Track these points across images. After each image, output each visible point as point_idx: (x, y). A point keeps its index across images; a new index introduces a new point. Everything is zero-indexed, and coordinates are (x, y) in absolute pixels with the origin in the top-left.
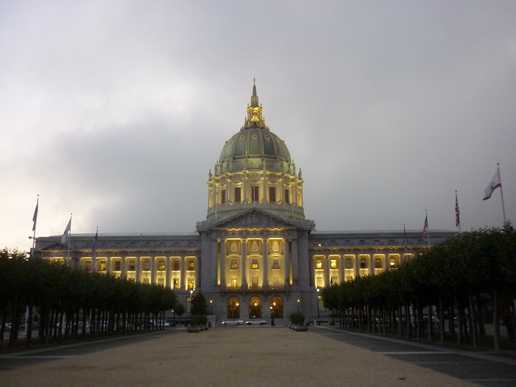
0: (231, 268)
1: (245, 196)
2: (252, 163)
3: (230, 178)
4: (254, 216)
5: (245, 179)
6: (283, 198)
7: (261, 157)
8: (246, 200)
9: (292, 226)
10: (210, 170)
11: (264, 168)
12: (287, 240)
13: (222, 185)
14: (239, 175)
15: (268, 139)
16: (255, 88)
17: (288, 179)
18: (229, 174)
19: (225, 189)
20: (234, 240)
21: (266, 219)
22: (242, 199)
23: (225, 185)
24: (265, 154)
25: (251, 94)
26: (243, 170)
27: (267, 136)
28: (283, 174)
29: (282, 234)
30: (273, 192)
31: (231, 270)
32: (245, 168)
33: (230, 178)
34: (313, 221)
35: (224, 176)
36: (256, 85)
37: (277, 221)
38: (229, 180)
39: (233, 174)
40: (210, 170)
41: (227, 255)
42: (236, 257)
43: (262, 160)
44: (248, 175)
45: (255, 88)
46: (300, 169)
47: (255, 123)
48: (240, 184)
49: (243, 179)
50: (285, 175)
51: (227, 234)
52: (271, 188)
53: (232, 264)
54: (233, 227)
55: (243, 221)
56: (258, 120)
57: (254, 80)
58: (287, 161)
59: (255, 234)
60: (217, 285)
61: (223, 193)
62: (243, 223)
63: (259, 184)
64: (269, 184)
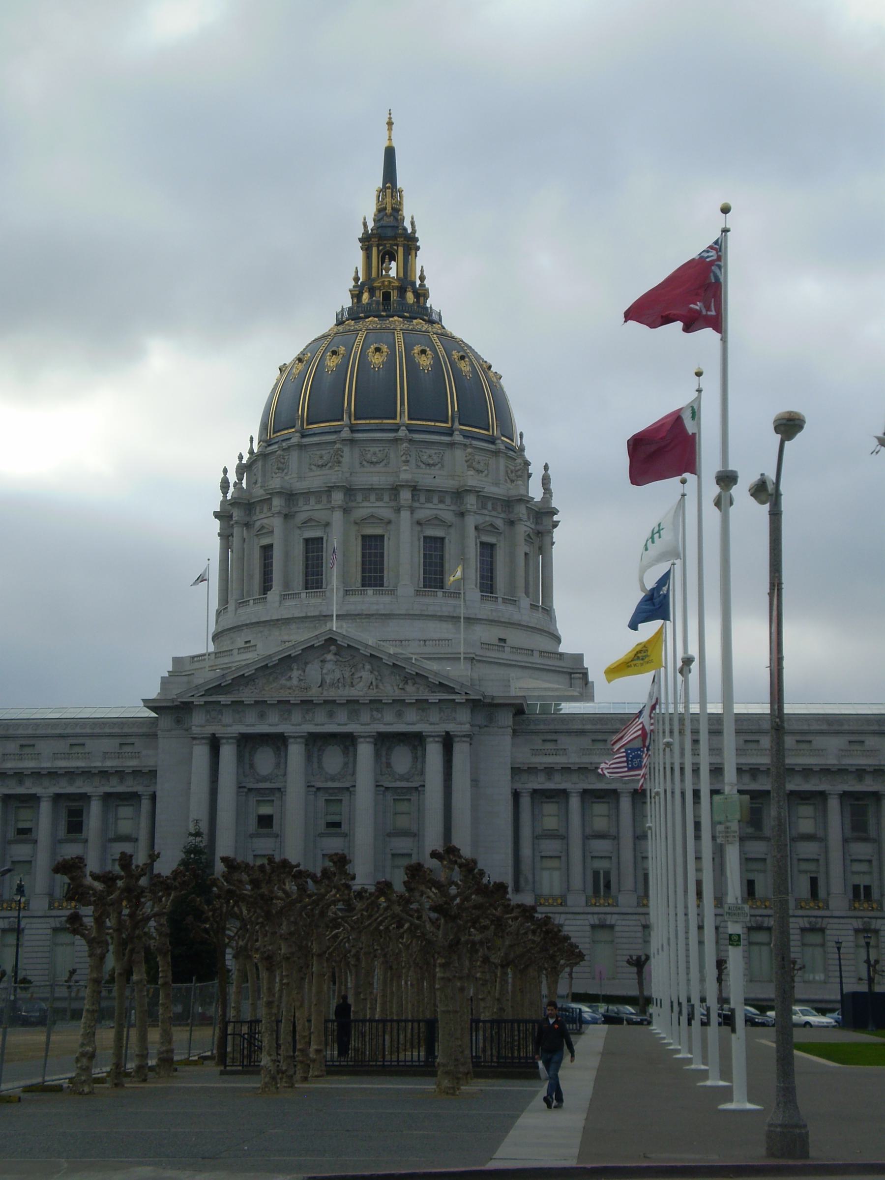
4: (330, 657)
9: (452, 690)
10: (225, 471)
15: (425, 362)
16: (390, 154)
21: (368, 667)
24: (410, 419)
25: (378, 182)
27: (423, 352)
34: (579, 658)
36: (395, 144)
40: (225, 471)
45: (390, 154)
46: (546, 468)
55: (295, 674)
57: (390, 124)
62: (295, 682)
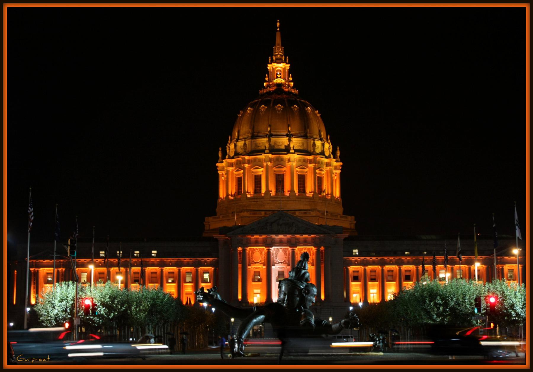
0: (254, 281)
1: (268, 187)
2: (275, 143)
3: (249, 162)
5: (267, 164)
6: (315, 189)
7: (287, 135)
8: (268, 191)
11: (292, 151)
12: (318, 250)
14: (260, 160)
17: (322, 163)
18: (247, 157)
19: (242, 175)
20: (257, 249)
22: (263, 190)
23: (242, 171)
26: (263, 151)
28: (315, 159)
29: (313, 243)
30: (302, 179)
31: (254, 283)
32: (266, 151)
33: (249, 162)
35: (240, 159)
37: (308, 229)
38: (246, 166)
39: (251, 157)
41: (249, 265)
42: (259, 268)
43: (290, 141)
44: (270, 160)
47: (279, 85)
48: (260, 171)
49: (265, 164)
50: (319, 158)
51: (249, 243)
52: (299, 176)
53: (254, 276)
54: (256, 234)
56: (283, 81)
58: (321, 140)
59: (281, 243)
60: (238, 300)
61: (240, 181)
63: (285, 171)
64: (297, 171)
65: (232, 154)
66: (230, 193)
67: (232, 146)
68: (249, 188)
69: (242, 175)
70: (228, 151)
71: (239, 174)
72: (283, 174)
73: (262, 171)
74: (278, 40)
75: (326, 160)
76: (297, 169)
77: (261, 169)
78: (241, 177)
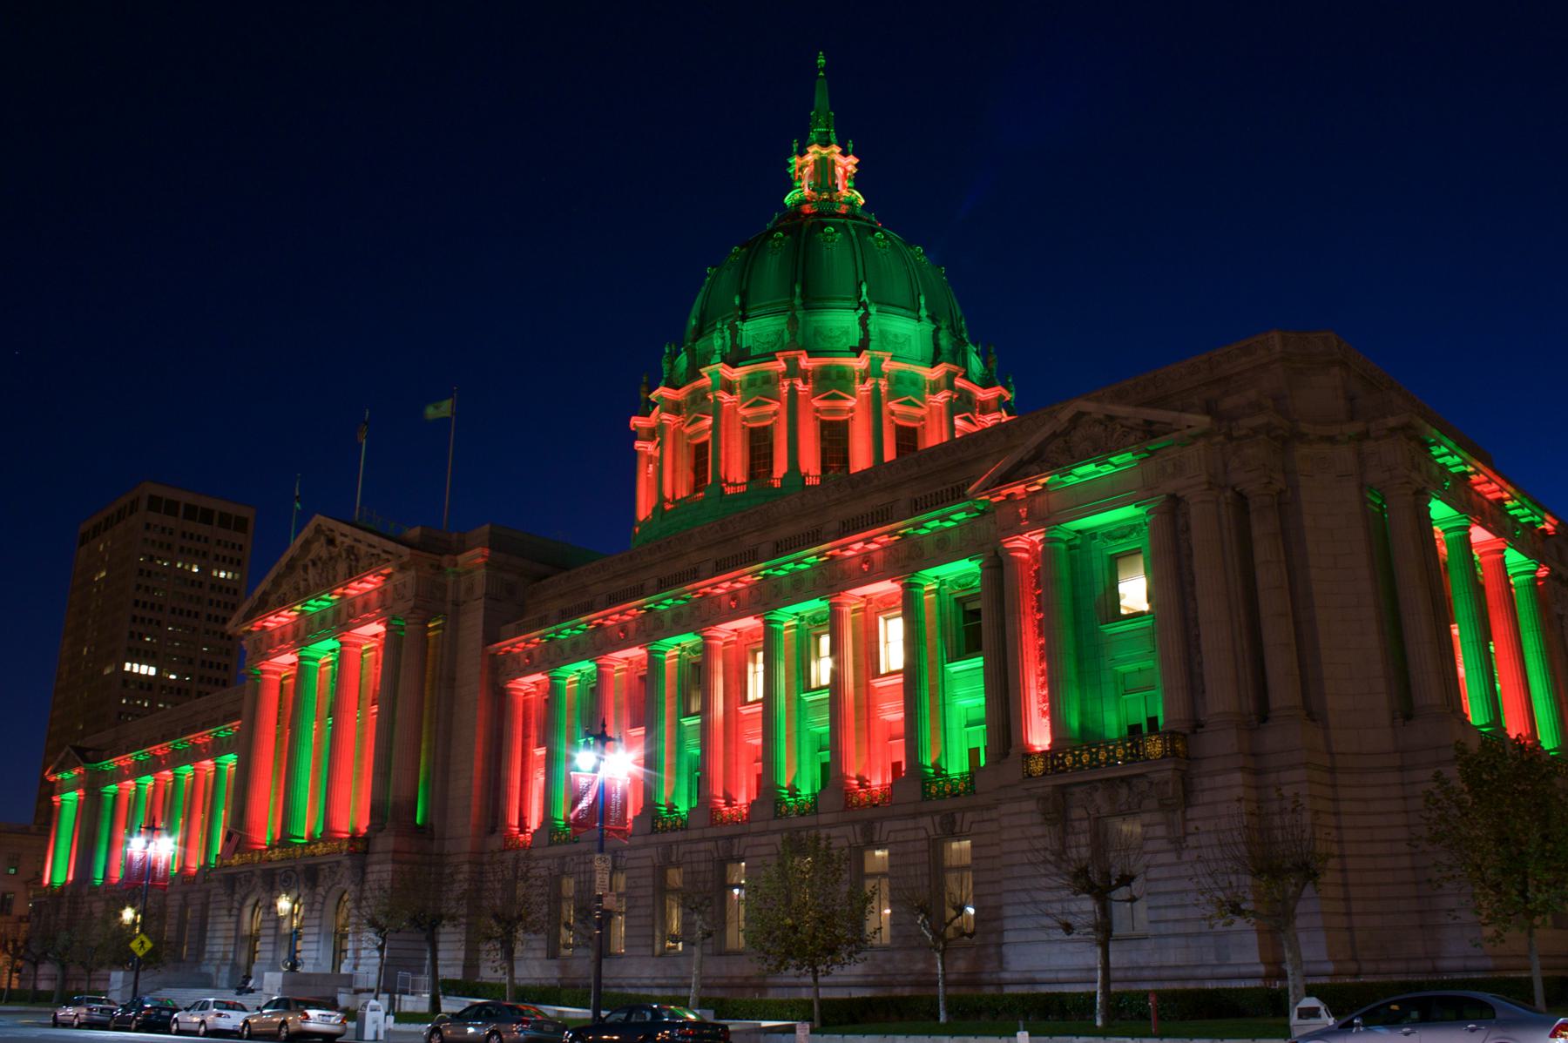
13: (696, 420)
19: (707, 436)
22: (780, 468)
23: (709, 421)
63: (852, 410)
64: (892, 413)
65: (682, 379)
66: (668, 495)
67: (683, 360)
68: (736, 468)
69: (707, 436)
70: (666, 367)
71: (700, 433)
72: (846, 422)
73: (776, 413)
74: (821, 98)
75: (982, 395)
76: (892, 405)
77: (775, 406)
78: (705, 444)
